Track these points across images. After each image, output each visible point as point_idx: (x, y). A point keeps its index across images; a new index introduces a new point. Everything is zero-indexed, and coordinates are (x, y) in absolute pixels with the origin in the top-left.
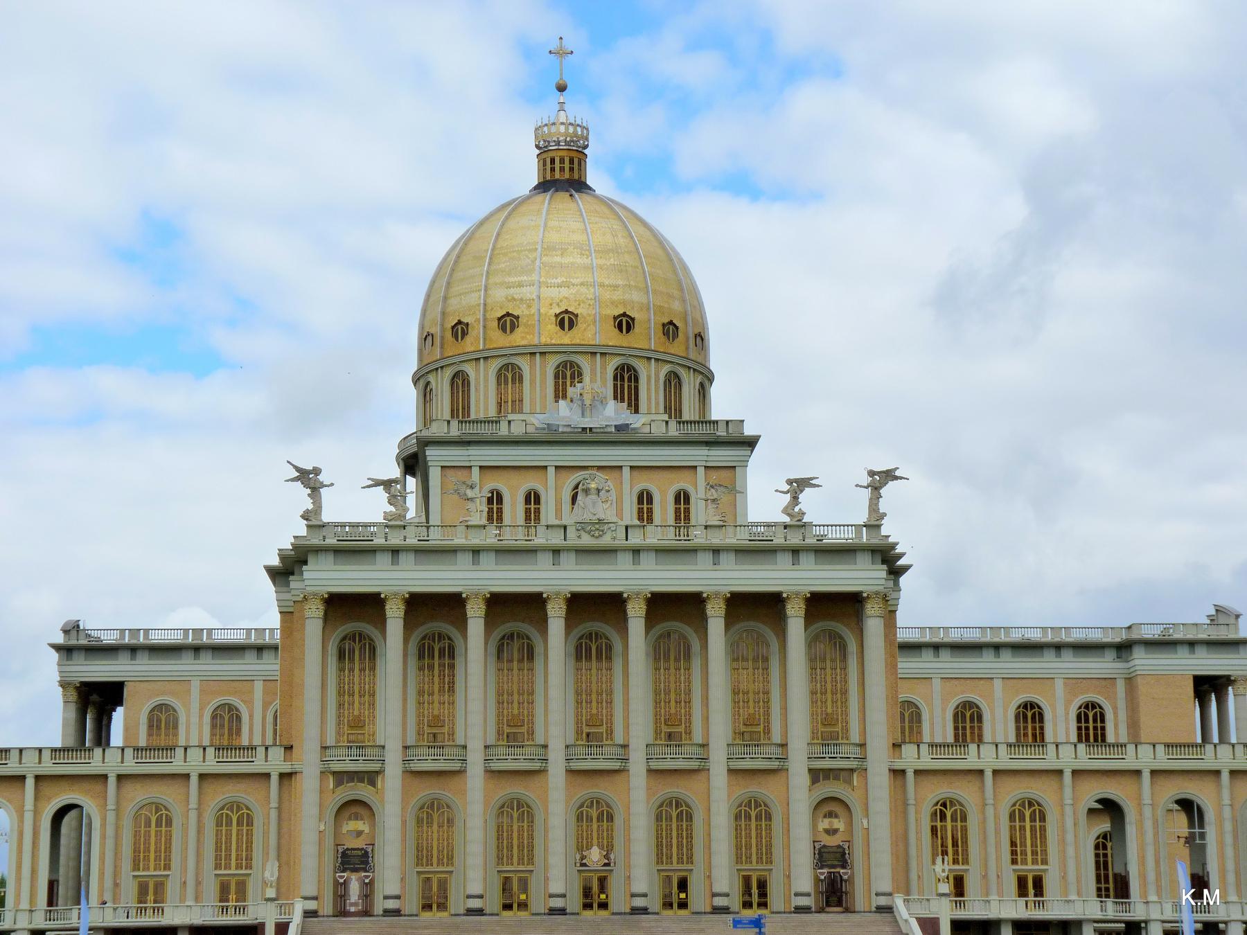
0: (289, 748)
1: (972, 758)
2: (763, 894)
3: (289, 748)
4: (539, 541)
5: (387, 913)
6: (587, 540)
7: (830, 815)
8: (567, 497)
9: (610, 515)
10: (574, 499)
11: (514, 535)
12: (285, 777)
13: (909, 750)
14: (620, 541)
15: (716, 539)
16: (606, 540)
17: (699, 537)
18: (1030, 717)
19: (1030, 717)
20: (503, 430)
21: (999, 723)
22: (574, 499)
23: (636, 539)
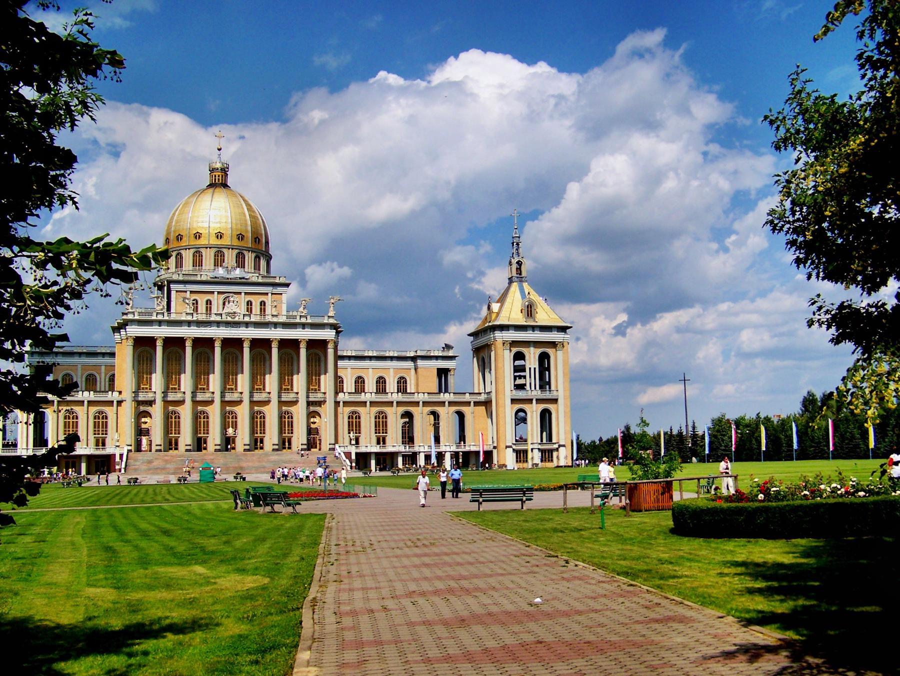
0: (120, 393)
1: (363, 397)
2: (290, 444)
3: (120, 393)
4: (212, 319)
5: (157, 451)
6: (229, 319)
7: (314, 417)
8: (221, 303)
9: (238, 311)
10: (224, 304)
11: (202, 317)
12: (120, 403)
13: (341, 395)
14: (241, 320)
15: (275, 320)
16: (237, 319)
17: (269, 318)
18: (381, 383)
19: (381, 383)
20: (198, 278)
21: (370, 385)
22: (224, 304)
23: (247, 319)
